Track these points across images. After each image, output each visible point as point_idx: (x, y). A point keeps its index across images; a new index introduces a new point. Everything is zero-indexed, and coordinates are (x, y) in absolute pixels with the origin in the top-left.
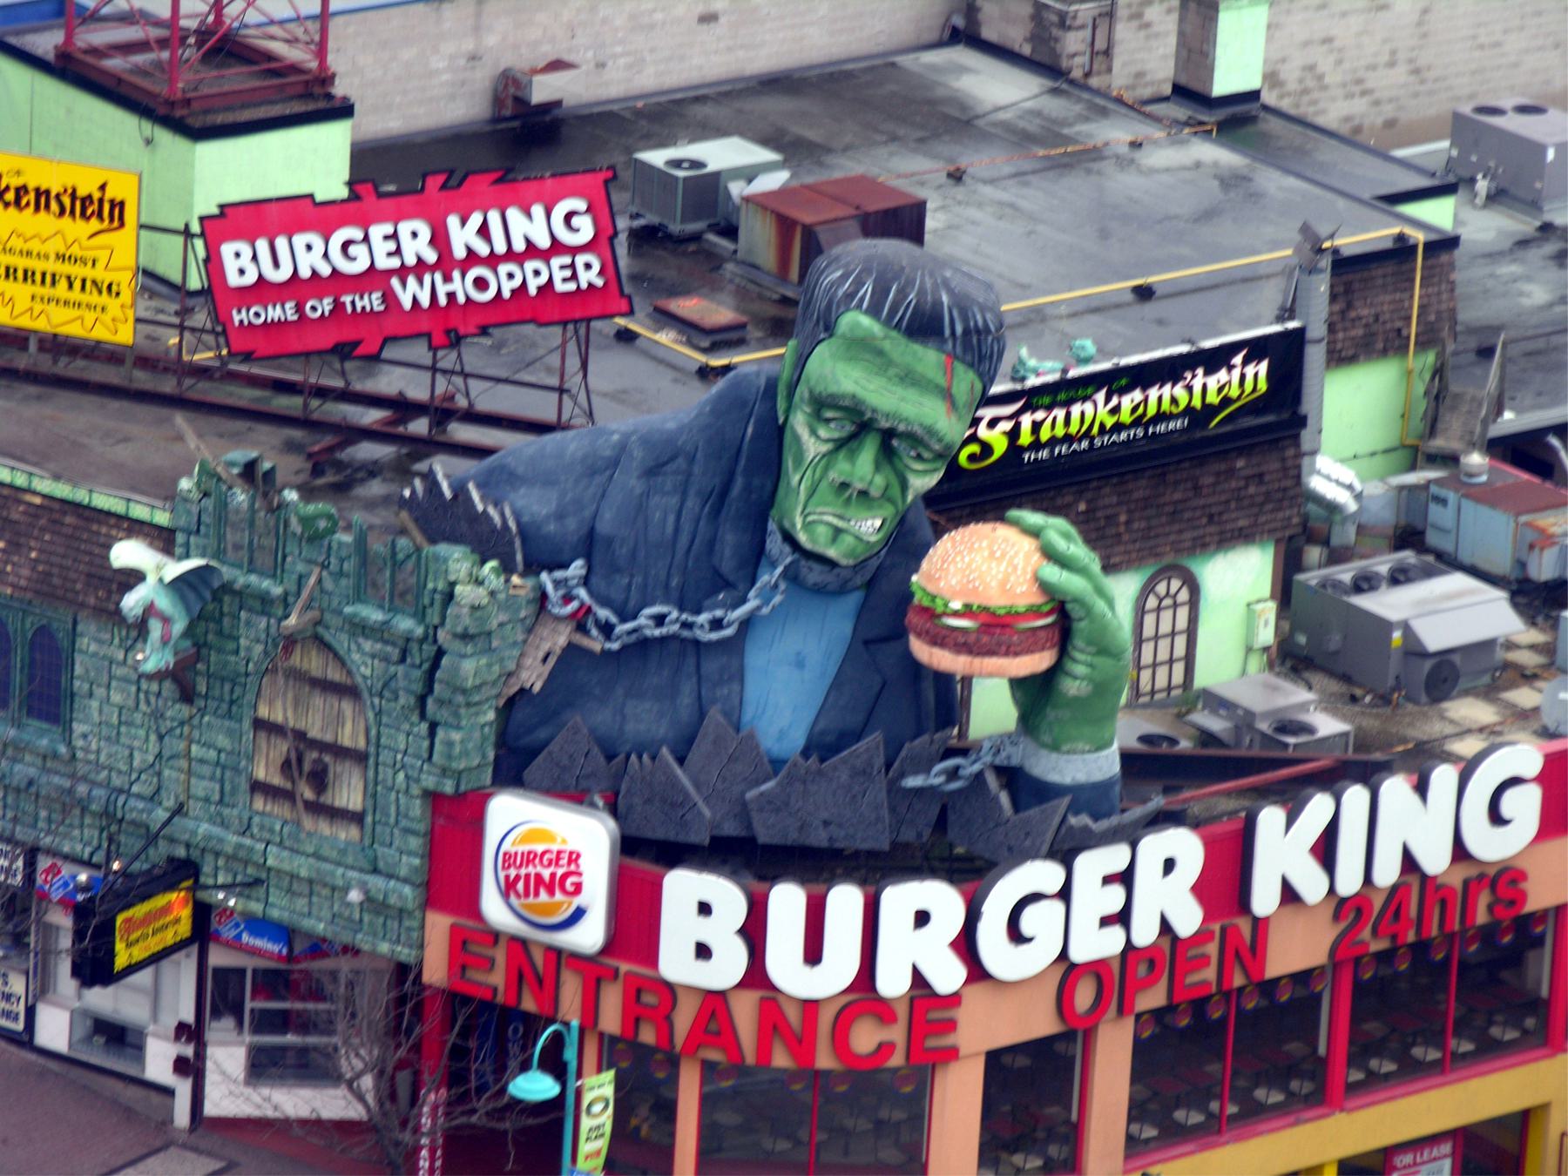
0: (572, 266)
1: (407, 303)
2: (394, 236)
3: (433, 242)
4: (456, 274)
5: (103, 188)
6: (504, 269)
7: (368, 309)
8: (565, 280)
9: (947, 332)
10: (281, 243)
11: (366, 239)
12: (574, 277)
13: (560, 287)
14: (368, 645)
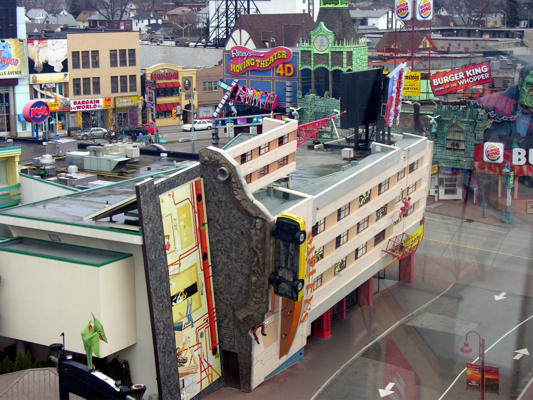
10: (442, 78)
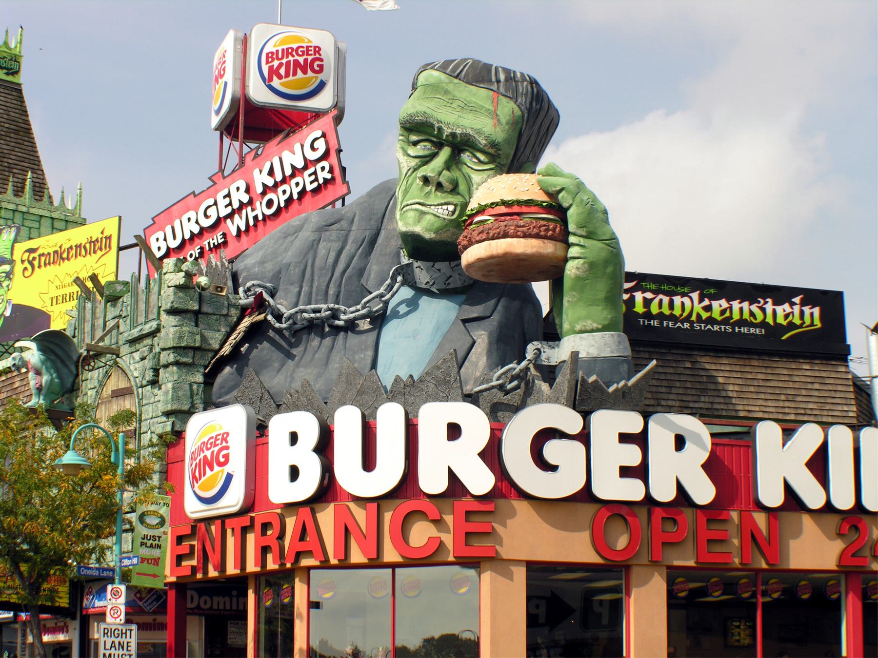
0: (315, 173)
1: (234, 233)
2: (228, 195)
3: (248, 191)
4: (258, 204)
5: (102, 233)
6: (280, 190)
7: (216, 244)
8: (311, 182)
9: (494, 79)
10: (177, 224)
11: (216, 204)
12: (316, 180)
13: (309, 188)
14: (137, 356)
